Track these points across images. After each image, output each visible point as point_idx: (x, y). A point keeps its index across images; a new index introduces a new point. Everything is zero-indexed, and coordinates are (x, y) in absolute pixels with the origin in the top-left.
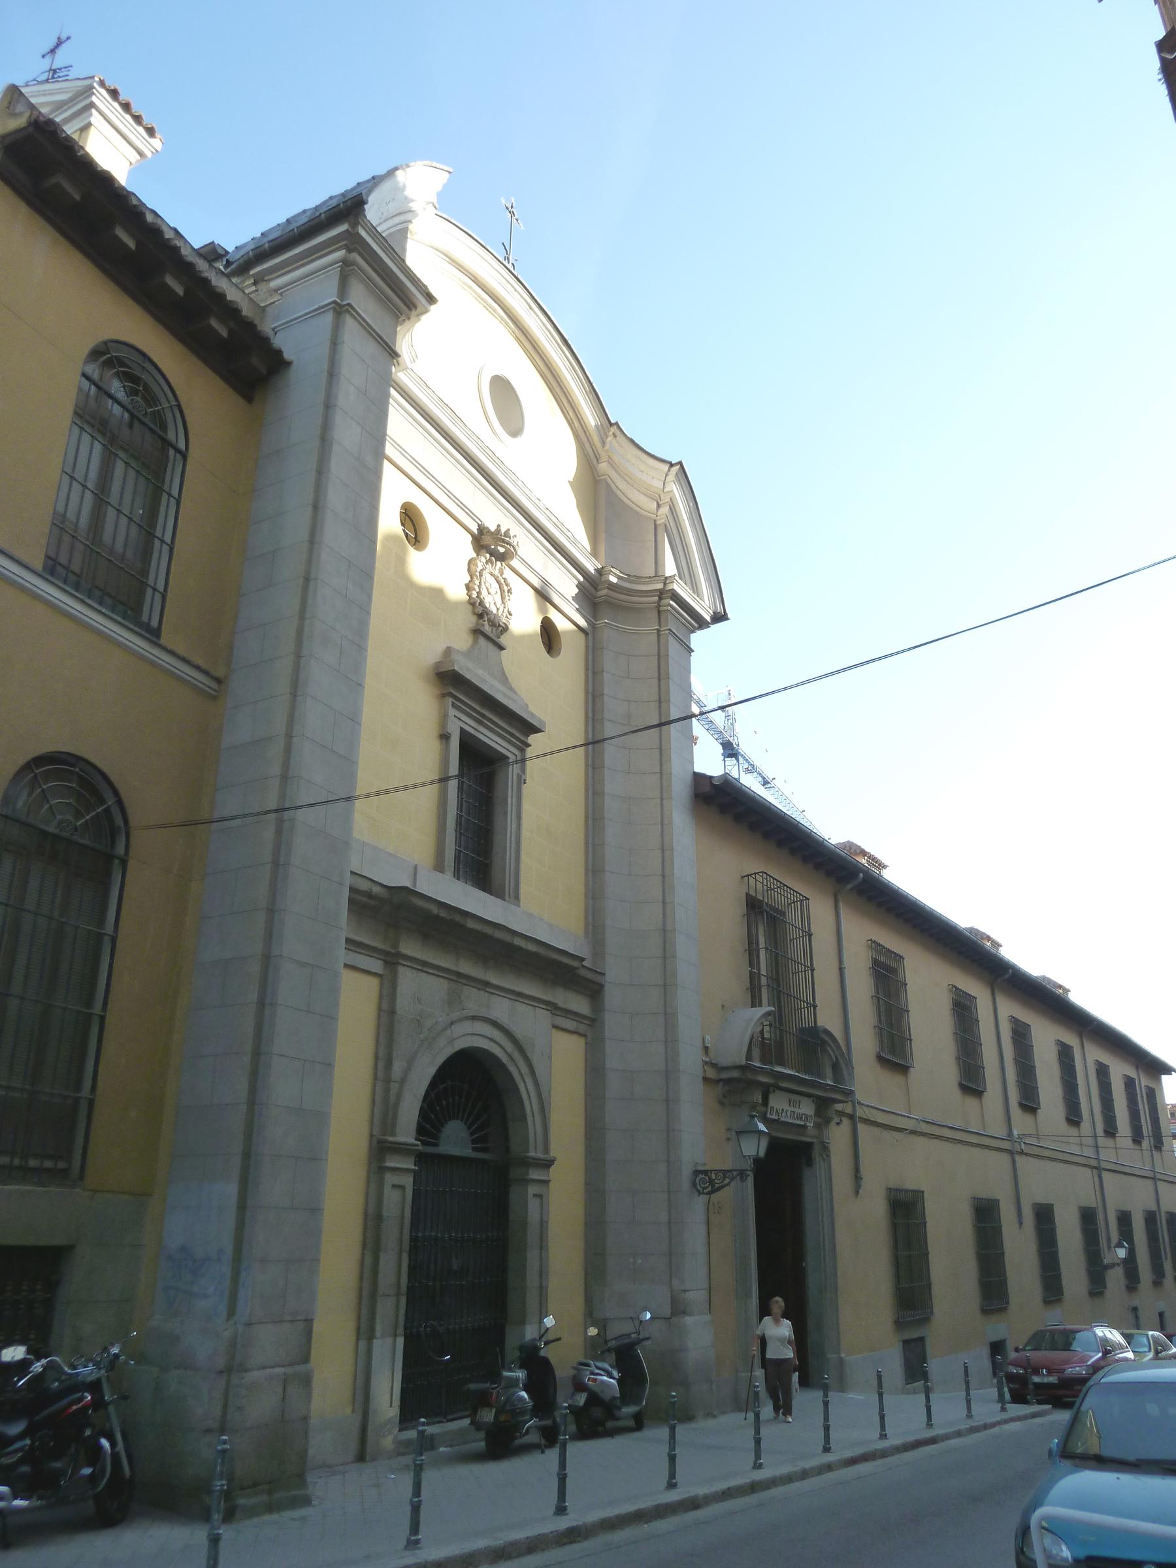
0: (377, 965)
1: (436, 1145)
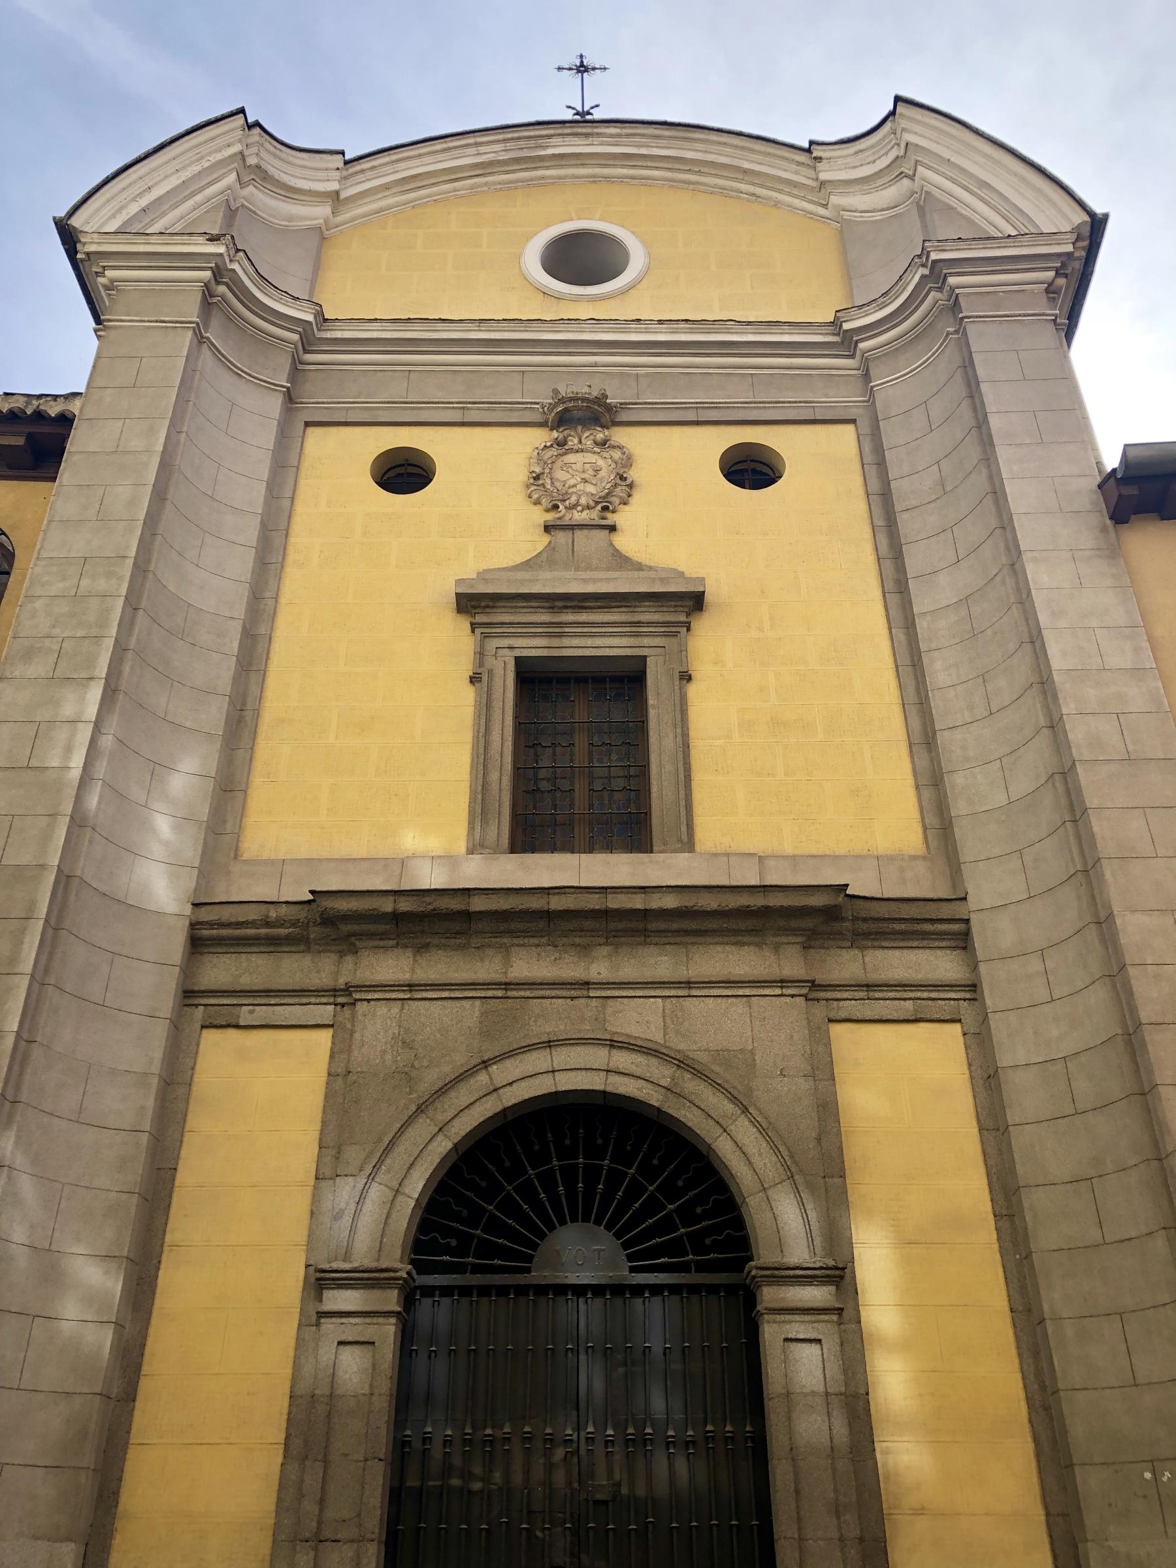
0: (326, 1012)
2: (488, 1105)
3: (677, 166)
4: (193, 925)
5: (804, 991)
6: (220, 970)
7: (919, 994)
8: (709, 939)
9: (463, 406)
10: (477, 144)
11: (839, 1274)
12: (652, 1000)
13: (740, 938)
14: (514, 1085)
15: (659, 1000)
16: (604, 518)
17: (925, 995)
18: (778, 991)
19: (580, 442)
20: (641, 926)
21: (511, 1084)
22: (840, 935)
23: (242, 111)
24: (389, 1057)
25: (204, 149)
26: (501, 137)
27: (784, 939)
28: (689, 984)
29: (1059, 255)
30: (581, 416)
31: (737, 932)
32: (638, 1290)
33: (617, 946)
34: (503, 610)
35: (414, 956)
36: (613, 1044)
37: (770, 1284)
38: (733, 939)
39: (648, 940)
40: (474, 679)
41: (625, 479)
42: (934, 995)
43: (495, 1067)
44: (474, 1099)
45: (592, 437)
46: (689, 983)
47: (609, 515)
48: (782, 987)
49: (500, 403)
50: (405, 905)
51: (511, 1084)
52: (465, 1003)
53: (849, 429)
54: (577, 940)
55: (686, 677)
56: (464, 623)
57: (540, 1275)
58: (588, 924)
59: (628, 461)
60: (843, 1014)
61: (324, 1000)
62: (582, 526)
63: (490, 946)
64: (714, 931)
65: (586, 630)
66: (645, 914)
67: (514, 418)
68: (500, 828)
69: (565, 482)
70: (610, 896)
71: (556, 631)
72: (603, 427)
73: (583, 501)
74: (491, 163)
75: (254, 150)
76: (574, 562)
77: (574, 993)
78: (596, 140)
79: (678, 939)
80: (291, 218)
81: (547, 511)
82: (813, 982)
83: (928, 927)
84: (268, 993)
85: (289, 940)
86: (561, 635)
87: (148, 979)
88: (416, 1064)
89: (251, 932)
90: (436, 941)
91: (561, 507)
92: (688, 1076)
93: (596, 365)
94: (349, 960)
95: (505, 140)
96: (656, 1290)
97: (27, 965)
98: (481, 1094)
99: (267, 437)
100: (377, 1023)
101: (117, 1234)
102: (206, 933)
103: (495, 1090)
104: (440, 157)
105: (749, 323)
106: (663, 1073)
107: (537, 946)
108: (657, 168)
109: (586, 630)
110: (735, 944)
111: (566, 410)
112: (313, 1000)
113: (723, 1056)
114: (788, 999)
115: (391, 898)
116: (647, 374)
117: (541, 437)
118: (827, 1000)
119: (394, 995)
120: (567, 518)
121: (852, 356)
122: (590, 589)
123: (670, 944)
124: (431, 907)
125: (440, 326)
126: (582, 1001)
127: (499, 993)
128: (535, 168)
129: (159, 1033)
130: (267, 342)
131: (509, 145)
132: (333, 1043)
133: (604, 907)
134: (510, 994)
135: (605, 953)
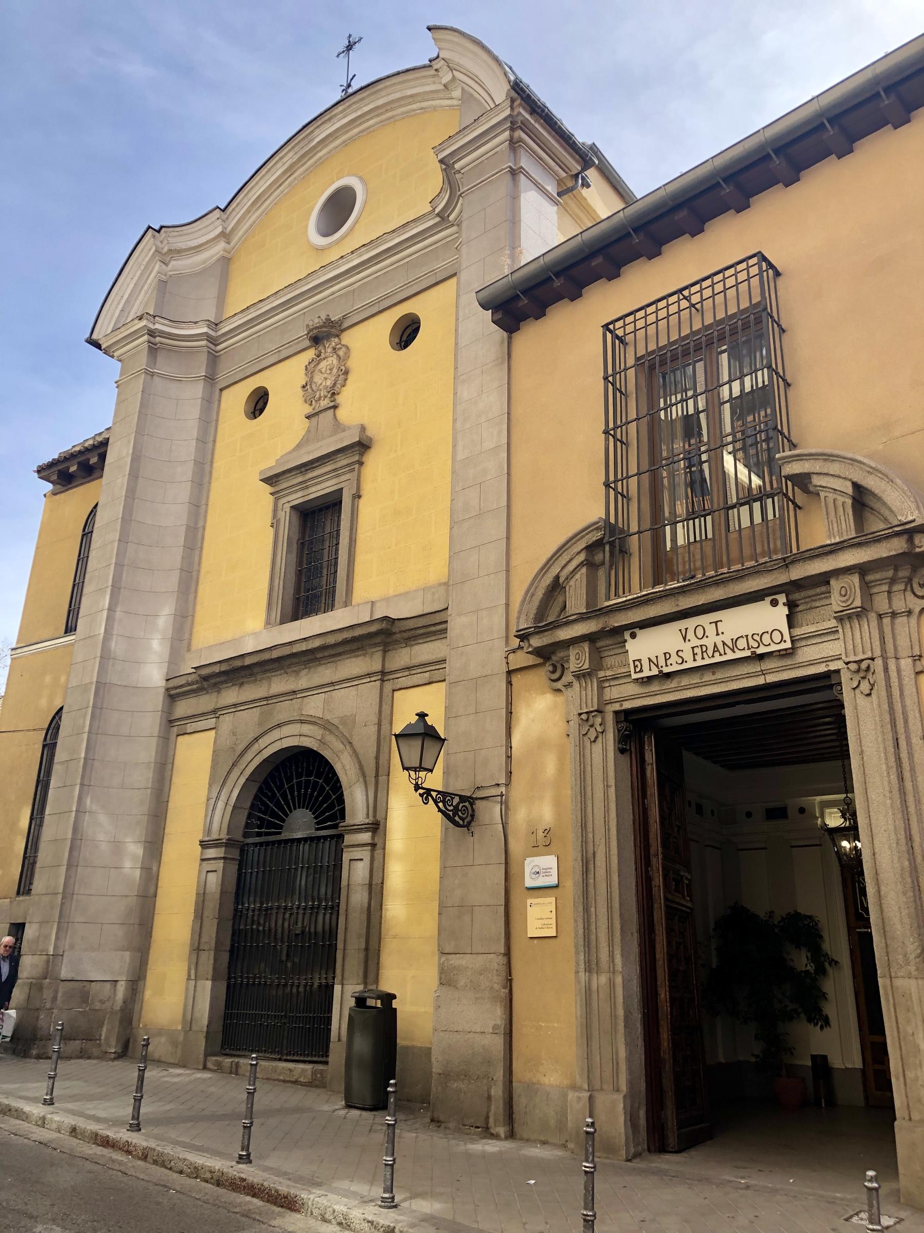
0: (211, 722)
1: (280, 833)
3: (380, 111)
4: (167, 690)
6: (183, 708)
7: (431, 668)
8: (344, 657)
9: (278, 350)
10: (281, 158)
11: (377, 827)
17: (434, 668)
18: (368, 680)
22: (397, 642)
23: (149, 227)
25: (140, 260)
26: (290, 147)
27: (374, 650)
28: (332, 684)
29: (505, 119)
31: (352, 651)
32: (319, 838)
33: (310, 668)
36: (302, 722)
37: (347, 833)
42: (437, 667)
52: (254, 710)
57: (285, 835)
60: (399, 687)
68: (277, 614)
71: (304, 485)
74: (291, 166)
75: (166, 242)
78: (335, 120)
80: (204, 262)
83: (433, 629)
86: (307, 487)
87: (149, 722)
89: (185, 689)
93: (333, 293)
95: (293, 148)
96: (325, 838)
97: (87, 729)
99: (193, 411)
101: (140, 833)
102: (172, 692)
104: (266, 177)
105: (393, 231)
106: (317, 732)
108: (372, 118)
110: (355, 656)
113: (344, 720)
117: (311, 354)
122: (310, 458)
125: (260, 305)
127: (265, 703)
128: (315, 154)
129: (154, 742)
130: (192, 352)
131: (296, 149)
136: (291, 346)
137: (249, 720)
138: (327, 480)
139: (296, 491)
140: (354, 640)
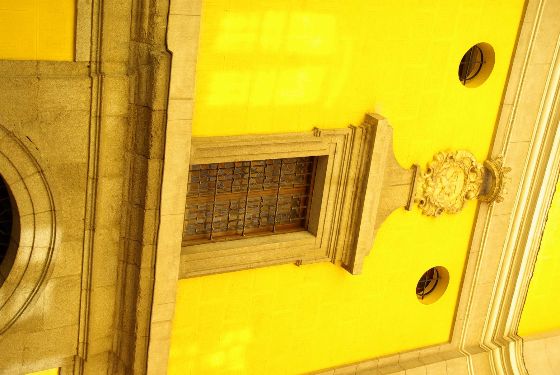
0: (85, 56)
2: (11, 175)
5: (80, 355)
8: (119, 298)
9: (515, 104)
12: (80, 268)
13: (118, 316)
14: (25, 190)
15: (80, 272)
16: (415, 202)
18: (81, 340)
19: (471, 182)
20: (131, 261)
21: (26, 188)
24: (49, 105)
27: (115, 340)
30: (489, 186)
33: (119, 243)
34: (362, 147)
35: (121, 116)
38: (118, 312)
39: (121, 262)
40: (316, 131)
41: (439, 213)
43: (39, 177)
44: (16, 166)
45: (473, 189)
46: (90, 290)
47: (417, 204)
48: (84, 343)
49: (510, 130)
50: (156, 118)
51: (26, 188)
53: (446, 338)
54: (124, 219)
55: (298, 263)
56: (357, 120)
58: (134, 229)
59: (451, 211)
61: (94, 55)
62: (412, 190)
63: (125, 164)
64: (124, 303)
65: (340, 200)
66: (138, 265)
67: (499, 138)
69: (445, 175)
70: (151, 247)
71: (342, 182)
72: (479, 195)
73: (429, 190)
76: (389, 185)
77: (88, 221)
79: (120, 281)
81: (428, 165)
82: (86, 360)
84: (101, 15)
85: (139, 29)
86: (339, 184)
88: (44, 125)
90: (131, 129)
91: (427, 176)
92: (27, 296)
93: (523, 188)
94: (122, 69)
98: (20, 171)
100: (74, 95)
103: (22, 179)
107: (123, 194)
109: (340, 200)
111: (494, 178)
112: (94, 46)
114: (76, 346)
115: (162, 108)
116: (509, 220)
118: (74, 365)
119: (94, 105)
120: (420, 179)
121: (493, 340)
123: (118, 275)
124: (154, 134)
126: (82, 226)
127: (91, 174)
132: (62, 62)
133: (144, 243)
134: (90, 181)
135: (114, 237)
136: (507, 125)
137: (70, 144)
138: (334, 216)
139: (341, 168)
140: (133, 336)
